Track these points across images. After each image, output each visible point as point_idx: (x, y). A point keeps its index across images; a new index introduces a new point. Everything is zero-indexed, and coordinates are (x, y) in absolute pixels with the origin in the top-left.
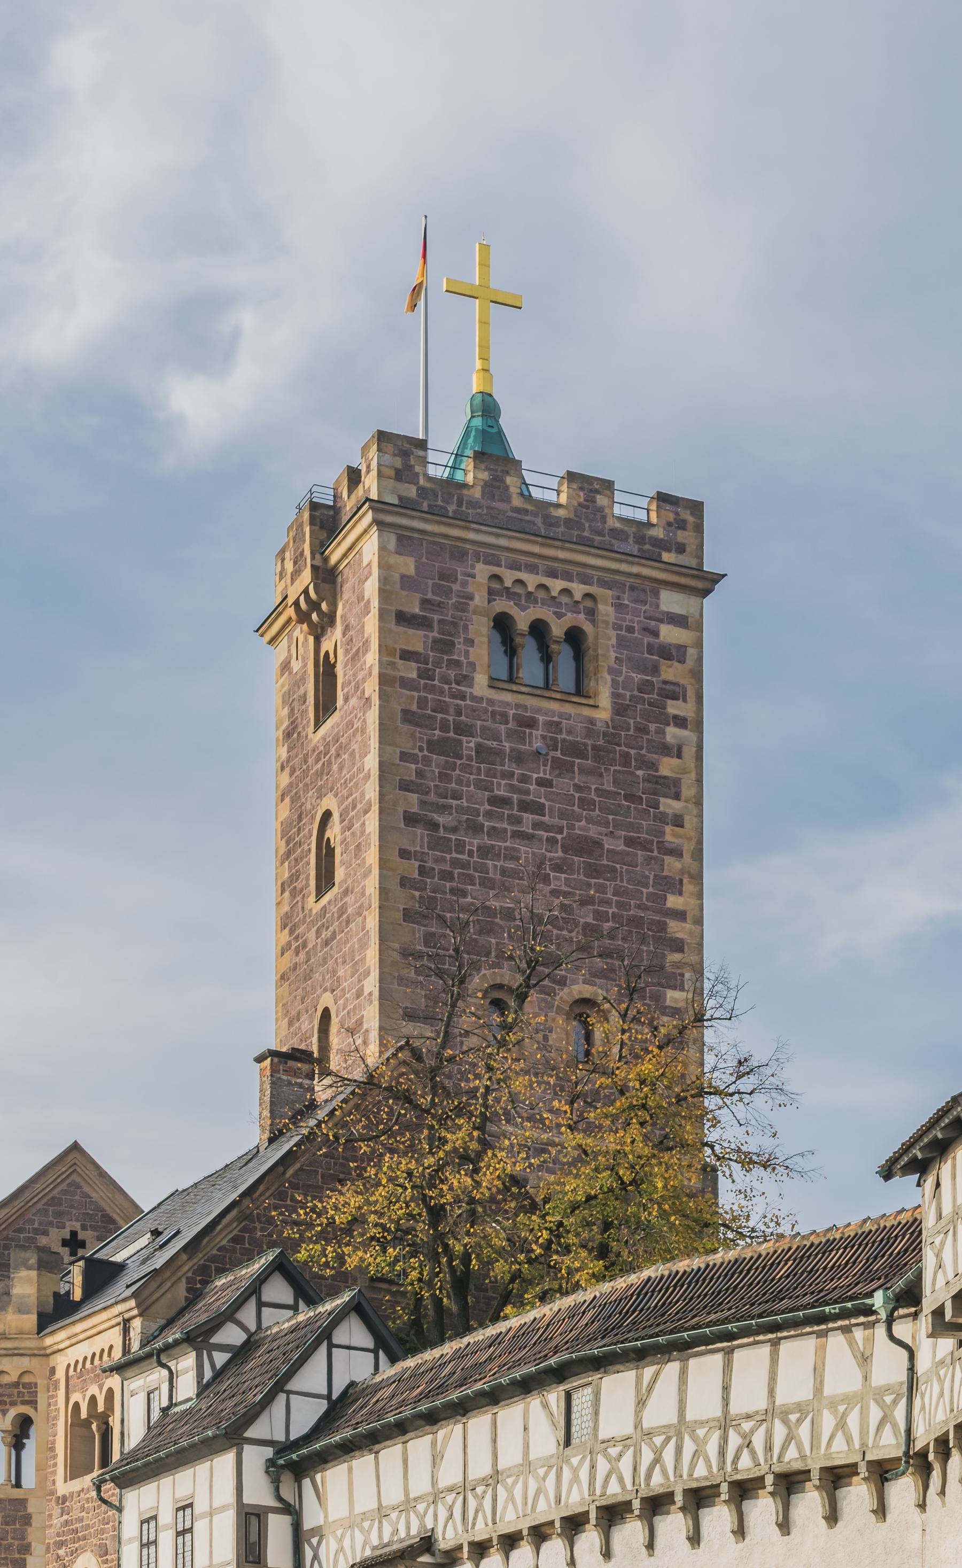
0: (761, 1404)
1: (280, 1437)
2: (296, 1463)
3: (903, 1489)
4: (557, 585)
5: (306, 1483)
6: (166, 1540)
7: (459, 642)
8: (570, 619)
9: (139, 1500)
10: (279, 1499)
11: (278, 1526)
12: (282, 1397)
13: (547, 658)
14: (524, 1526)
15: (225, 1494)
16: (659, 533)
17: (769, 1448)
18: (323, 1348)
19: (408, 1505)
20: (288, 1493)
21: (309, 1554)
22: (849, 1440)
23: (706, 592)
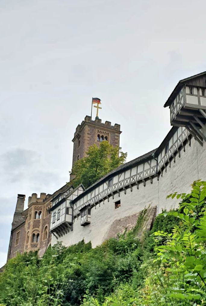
0: (136, 174)
1: (71, 199)
2: (73, 202)
3: (155, 180)
4: (105, 132)
5: (74, 205)
6: (57, 215)
7: (94, 136)
8: (106, 135)
9: (52, 213)
10: (71, 206)
11: (70, 210)
12: (72, 195)
13: (103, 139)
14: (103, 198)
15: (65, 206)
16: (115, 127)
17: (136, 178)
18: (77, 190)
19: (88, 201)
20: (72, 206)
21: (74, 212)
22: (148, 174)
23: (120, 133)
